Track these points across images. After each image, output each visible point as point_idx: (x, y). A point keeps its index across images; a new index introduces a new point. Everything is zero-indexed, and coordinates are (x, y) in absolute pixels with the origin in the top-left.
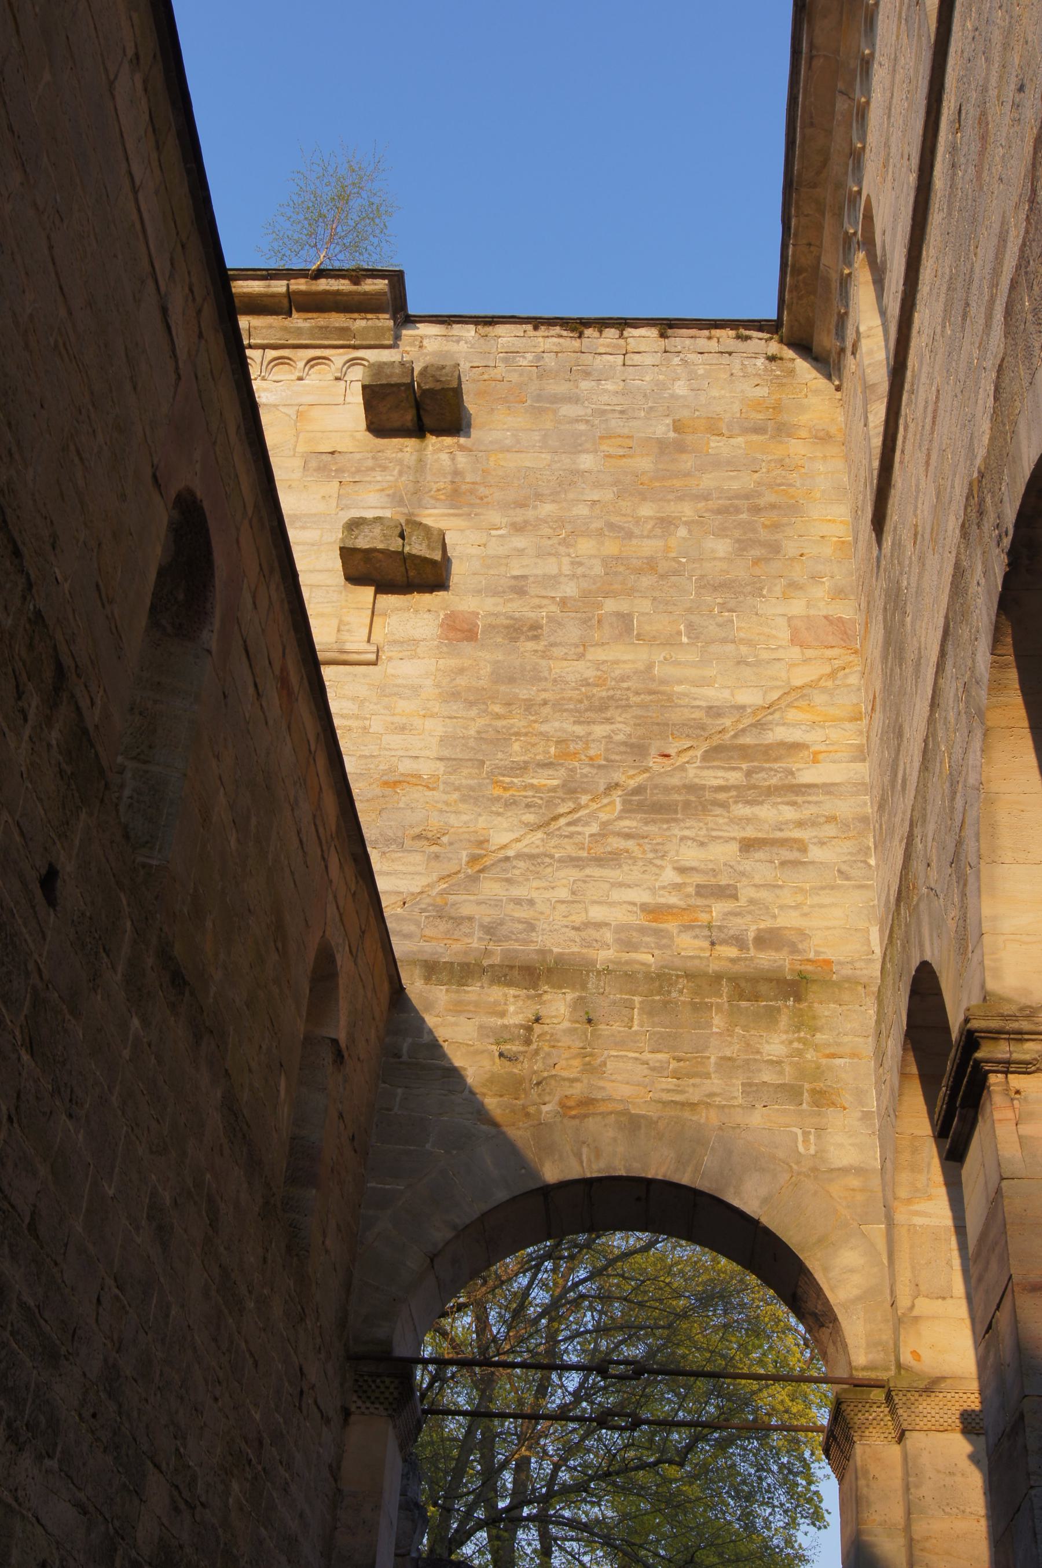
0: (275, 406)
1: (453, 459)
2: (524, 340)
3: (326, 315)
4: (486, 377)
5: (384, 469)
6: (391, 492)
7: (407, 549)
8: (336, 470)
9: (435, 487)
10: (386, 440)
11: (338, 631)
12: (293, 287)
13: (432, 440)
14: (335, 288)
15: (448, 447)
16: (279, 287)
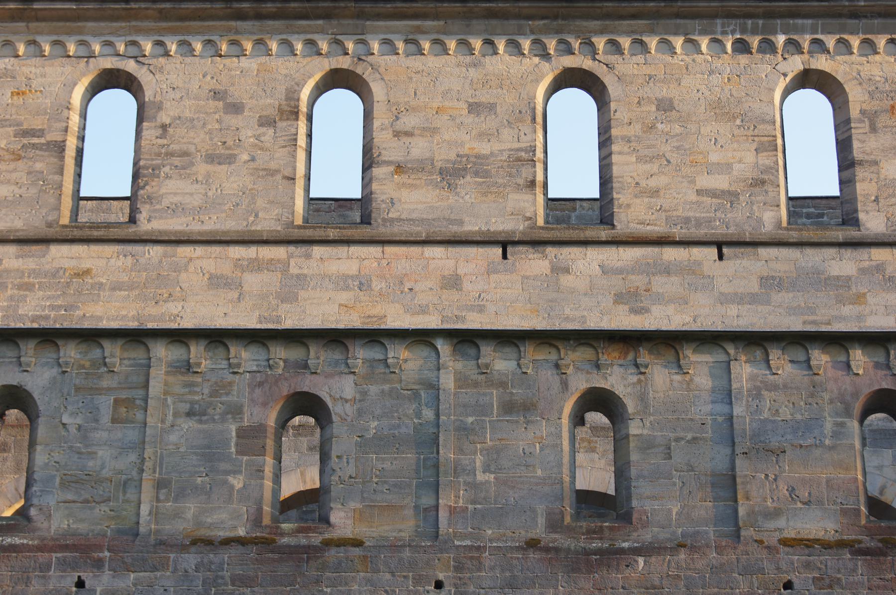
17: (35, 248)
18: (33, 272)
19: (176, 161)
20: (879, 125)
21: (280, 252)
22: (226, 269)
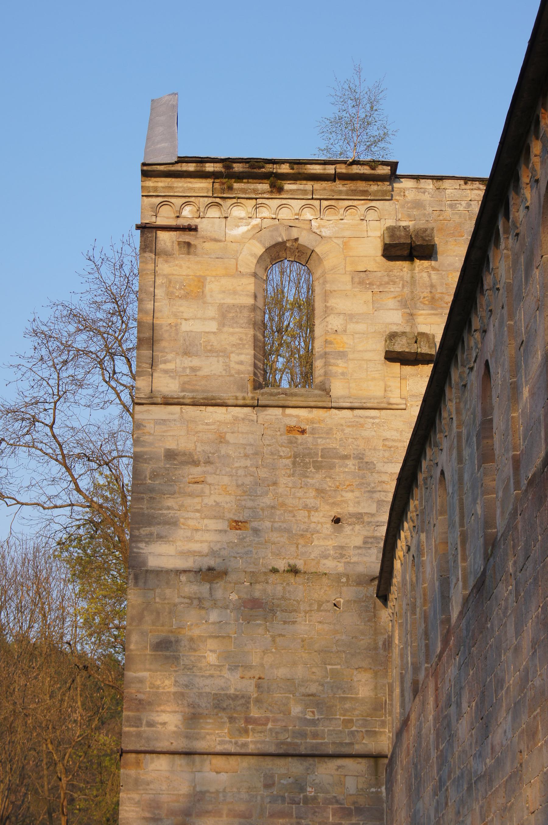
0: (330, 238)
1: (430, 277)
2: (460, 192)
3: (355, 182)
4: (441, 218)
5: (394, 283)
6: (399, 299)
7: (419, 350)
8: (369, 284)
9: (422, 295)
10: (393, 262)
11: (385, 391)
12: (338, 171)
13: (417, 262)
14: (362, 172)
15: (427, 268)
16: (330, 170)
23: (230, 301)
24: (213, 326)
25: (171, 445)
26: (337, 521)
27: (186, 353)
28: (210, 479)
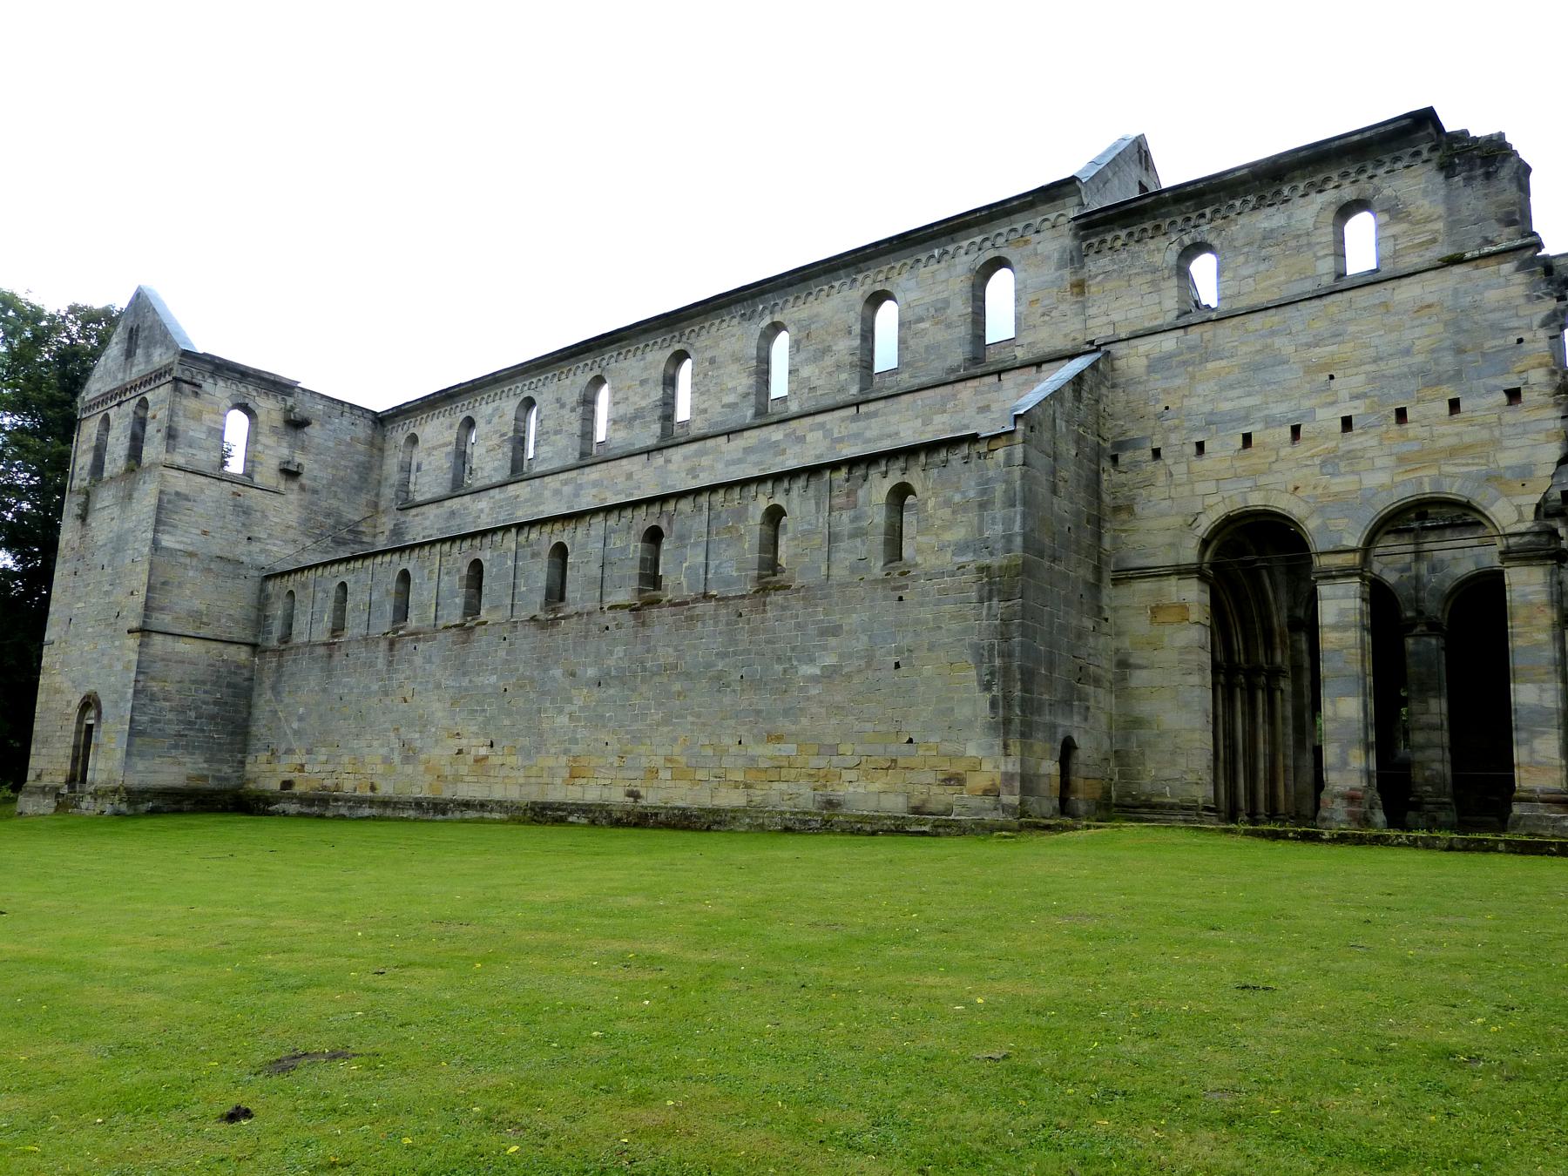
17: (503, 488)
18: (504, 500)
19: (545, 437)
20: (801, 346)
21: (574, 474)
22: (558, 485)
23: (212, 425)
24: (203, 436)
25: (178, 490)
26: (249, 539)
27: (190, 447)
28: (195, 509)
